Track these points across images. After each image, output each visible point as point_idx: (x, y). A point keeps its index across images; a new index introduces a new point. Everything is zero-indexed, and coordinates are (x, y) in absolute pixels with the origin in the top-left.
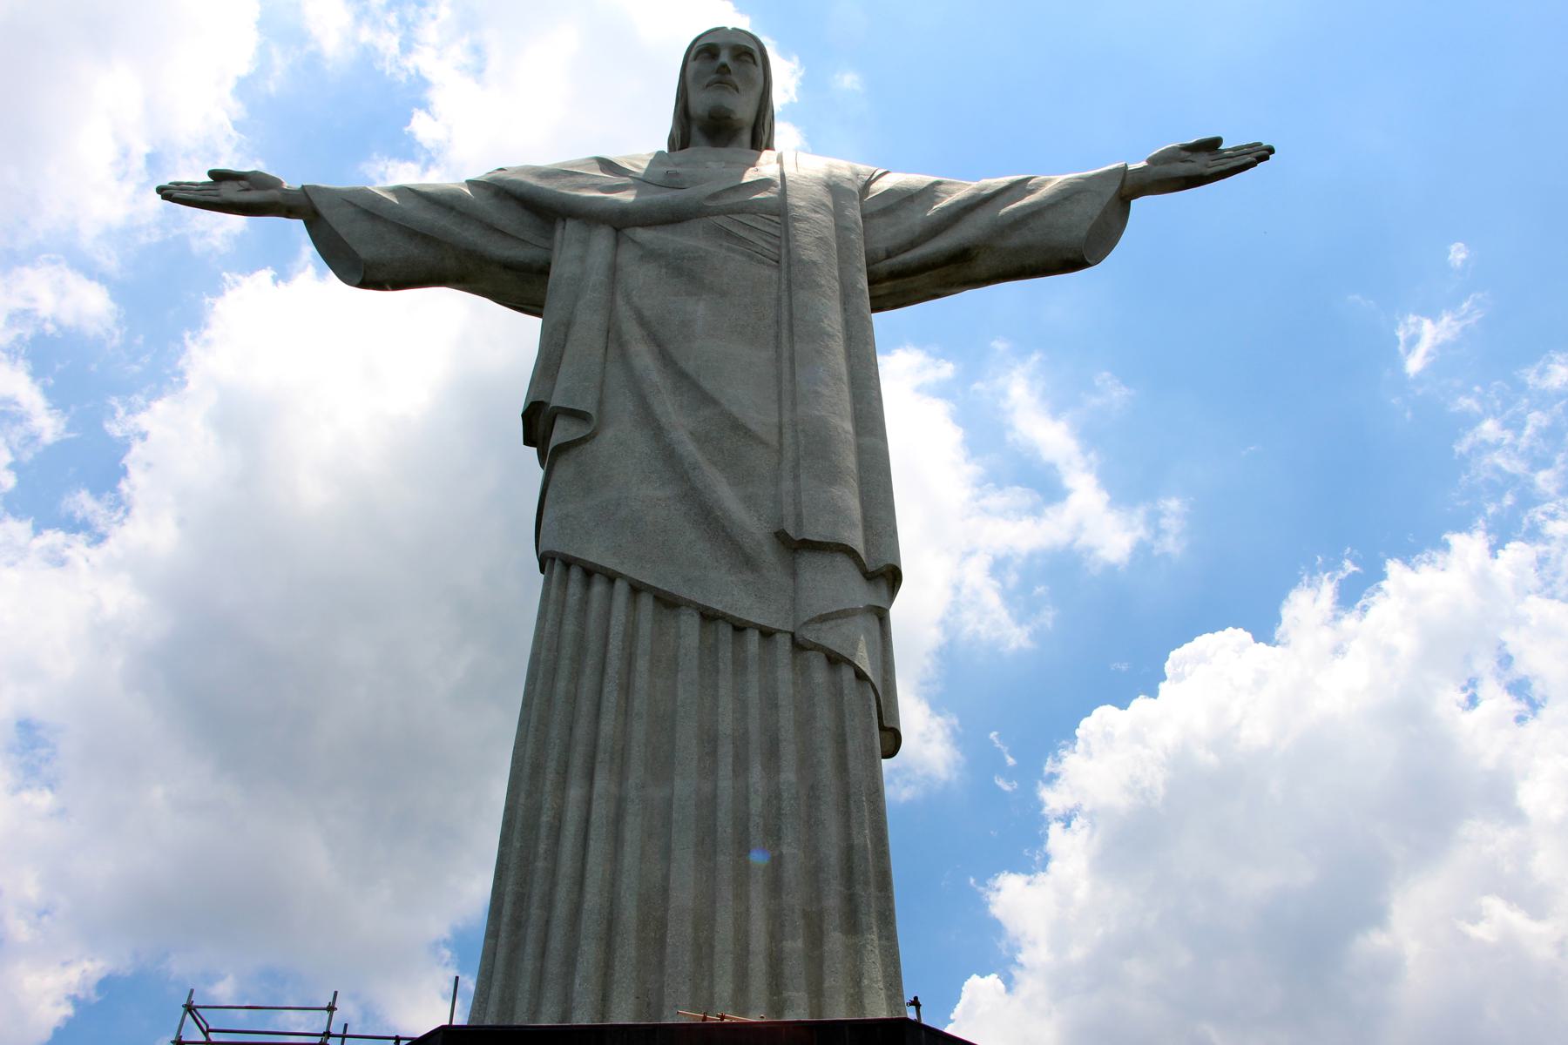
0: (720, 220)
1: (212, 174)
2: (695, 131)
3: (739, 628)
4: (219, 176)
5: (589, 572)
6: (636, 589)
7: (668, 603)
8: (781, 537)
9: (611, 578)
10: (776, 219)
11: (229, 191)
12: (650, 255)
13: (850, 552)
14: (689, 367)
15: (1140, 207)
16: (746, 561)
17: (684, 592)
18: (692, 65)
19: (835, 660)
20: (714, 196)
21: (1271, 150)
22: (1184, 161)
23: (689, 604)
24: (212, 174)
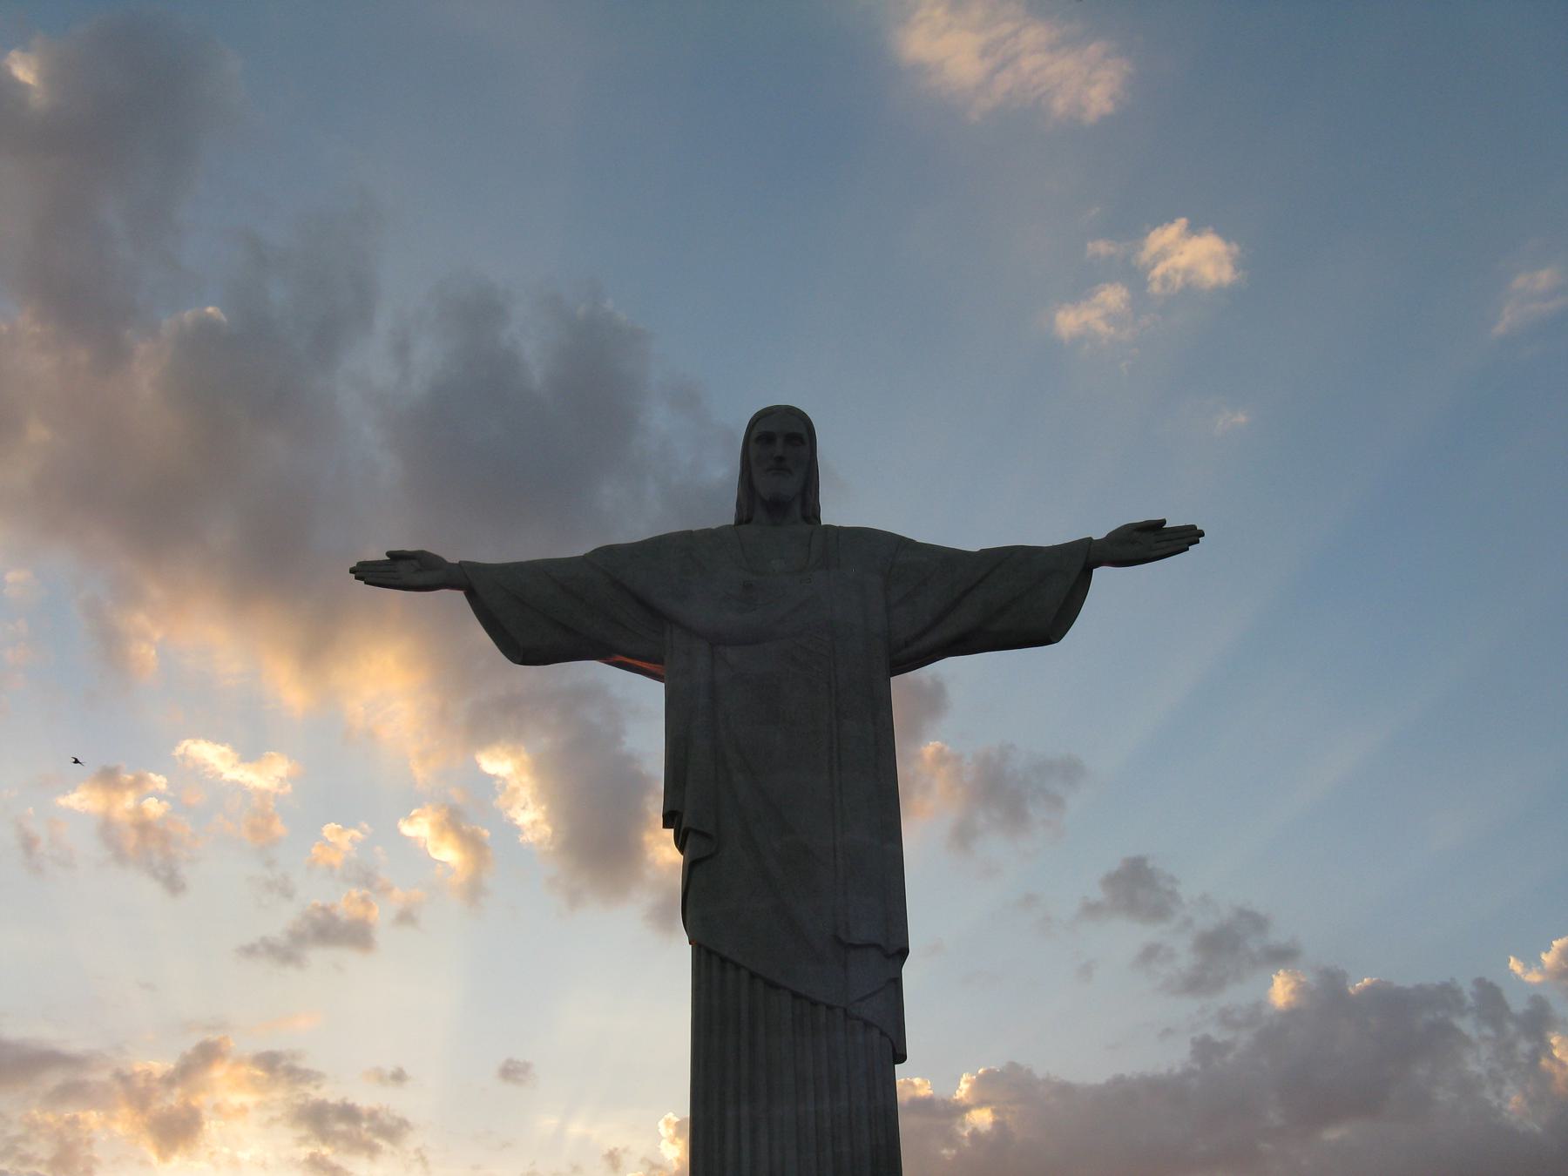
1: (388, 554)
3: (815, 1004)
4: (395, 557)
5: (724, 960)
6: (753, 976)
7: (771, 985)
9: (738, 967)
13: (877, 946)
19: (868, 1025)
21: (1202, 534)
24: (388, 554)
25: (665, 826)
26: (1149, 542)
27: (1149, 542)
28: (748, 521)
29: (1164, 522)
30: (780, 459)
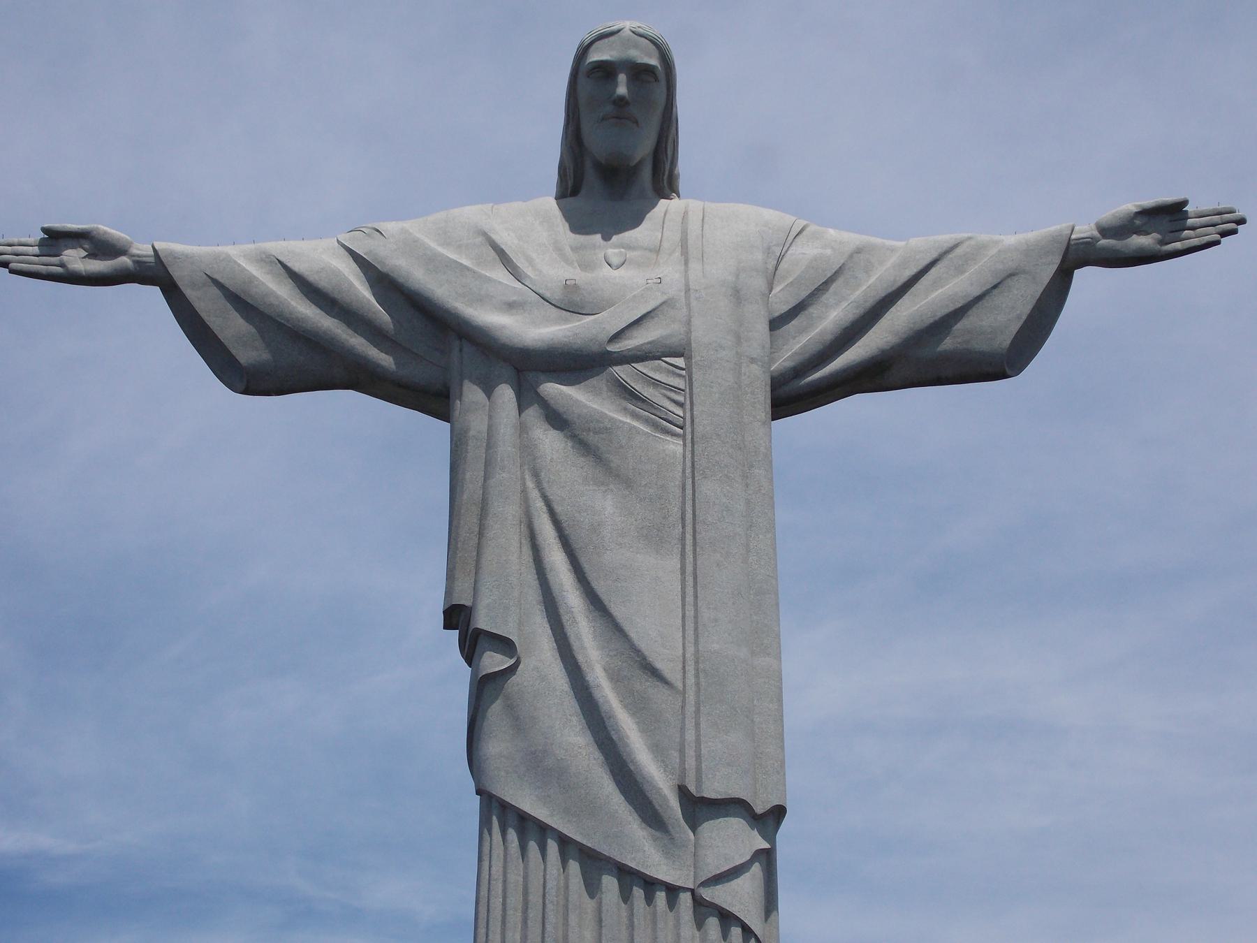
0: (621, 371)
2: (588, 164)
3: (650, 884)
6: (565, 842)
8: (683, 791)
10: (680, 362)
11: (75, 258)
12: (557, 419)
14: (600, 587)
15: (1085, 278)
16: (651, 816)
17: (605, 849)
18: (585, 86)
20: (616, 337)
21: (1241, 221)
22: (1139, 232)
23: (608, 860)
24: (45, 230)
25: (448, 626)
26: (1160, 231)
27: (1160, 231)
28: (575, 192)
29: (1185, 203)
30: (621, 102)
